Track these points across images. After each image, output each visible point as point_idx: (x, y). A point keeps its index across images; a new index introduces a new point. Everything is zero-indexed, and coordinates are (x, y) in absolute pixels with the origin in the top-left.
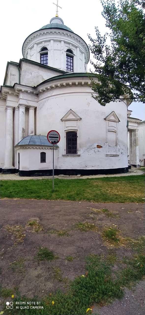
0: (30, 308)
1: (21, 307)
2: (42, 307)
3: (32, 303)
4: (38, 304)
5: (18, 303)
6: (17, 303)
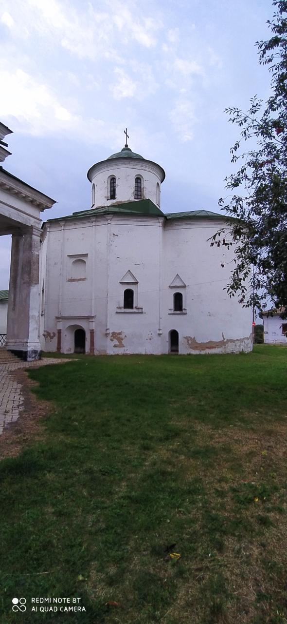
0: (59, 609)
1: (42, 609)
5: (35, 601)
6: (33, 599)
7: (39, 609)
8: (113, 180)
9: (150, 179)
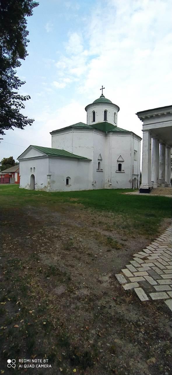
2: (50, 366)
3: (38, 360)
4: (45, 361)
5: (21, 361)
7: (23, 366)
8: (94, 113)
9: (111, 111)
